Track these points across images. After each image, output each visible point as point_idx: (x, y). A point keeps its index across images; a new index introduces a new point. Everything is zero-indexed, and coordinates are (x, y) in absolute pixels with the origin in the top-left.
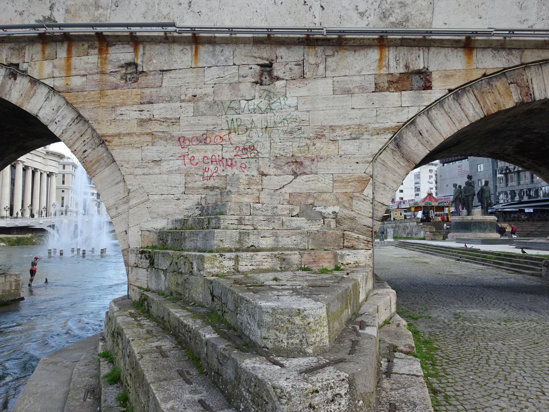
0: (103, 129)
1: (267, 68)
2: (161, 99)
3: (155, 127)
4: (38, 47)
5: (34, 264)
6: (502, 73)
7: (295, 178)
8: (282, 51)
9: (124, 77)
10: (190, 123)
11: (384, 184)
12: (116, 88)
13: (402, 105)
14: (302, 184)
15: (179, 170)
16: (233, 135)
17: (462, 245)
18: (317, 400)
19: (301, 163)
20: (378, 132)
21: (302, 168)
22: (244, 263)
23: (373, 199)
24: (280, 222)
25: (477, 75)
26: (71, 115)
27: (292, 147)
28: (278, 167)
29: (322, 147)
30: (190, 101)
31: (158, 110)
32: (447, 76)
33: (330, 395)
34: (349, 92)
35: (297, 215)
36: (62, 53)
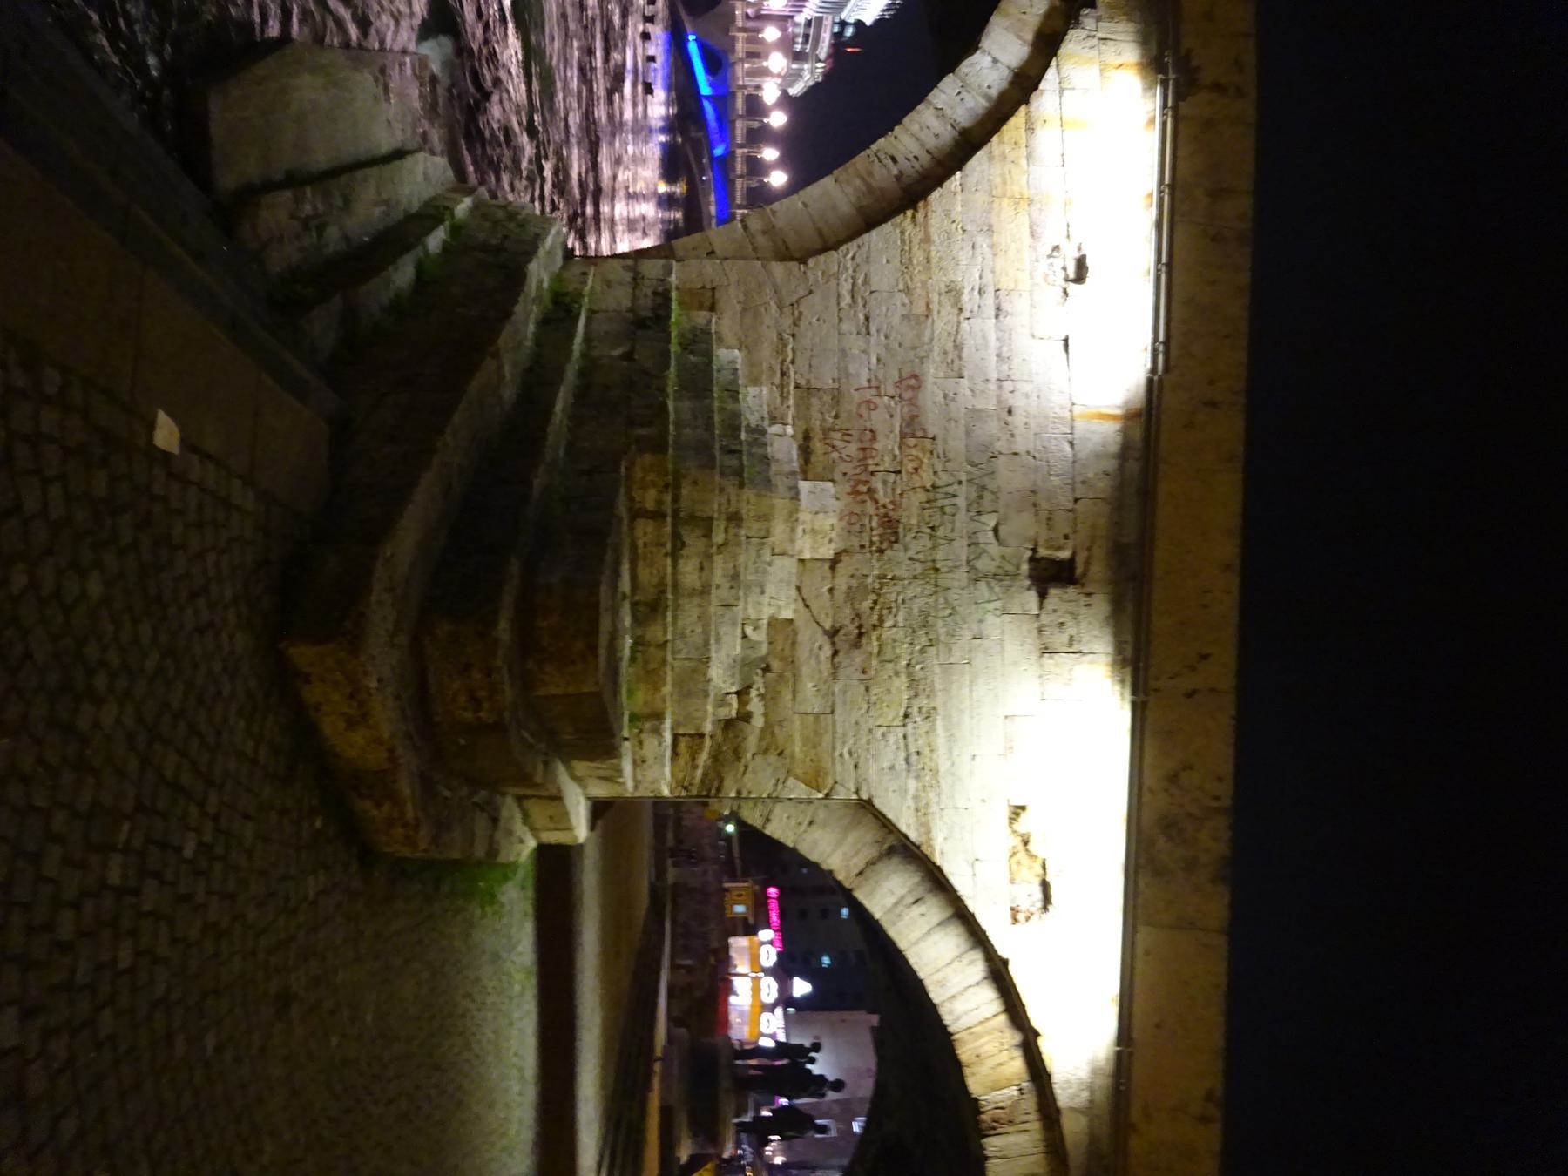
7: (826, 632)
11: (811, 823)
12: (1032, 234)
15: (848, 375)
16: (922, 496)
17: (659, 1052)
18: (477, 675)
19: (857, 645)
21: (847, 646)
22: (650, 529)
23: (777, 800)
24: (732, 601)
28: (851, 595)
30: (999, 402)
33: (482, 694)
35: (744, 636)
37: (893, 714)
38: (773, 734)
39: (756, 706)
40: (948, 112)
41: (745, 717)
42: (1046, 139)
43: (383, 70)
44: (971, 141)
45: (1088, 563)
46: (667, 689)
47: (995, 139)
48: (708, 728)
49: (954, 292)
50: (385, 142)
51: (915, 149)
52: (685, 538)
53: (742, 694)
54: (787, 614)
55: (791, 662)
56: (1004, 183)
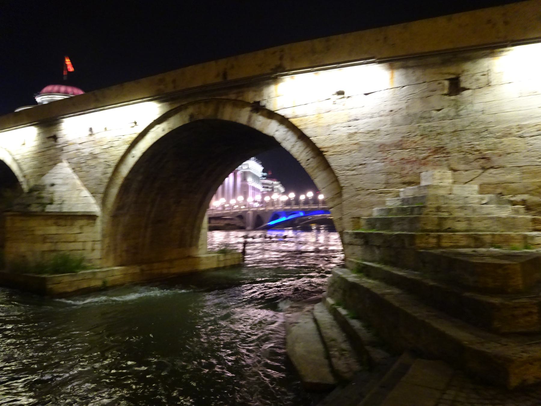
28: (468, 163)
30: (387, 116)
37: (520, 143)
38: (531, 191)
39: (519, 198)
40: (292, 144)
41: (523, 202)
42: (298, 111)
43: (291, 323)
44: (302, 136)
45: (449, 74)
46: (512, 233)
47: (300, 128)
48: (529, 217)
49: (350, 135)
50: (311, 325)
51: (304, 153)
52: (447, 227)
53: (514, 203)
54: (476, 187)
55: (498, 185)
56: (313, 123)
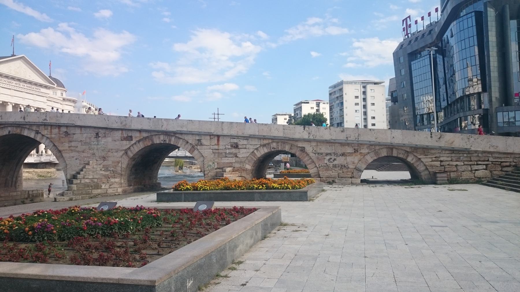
0: (60, 148)
1: (97, 134)
2: (73, 141)
3: (72, 148)
4: (43, 127)
5: (50, 186)
6: (147, 137)
8: (100, 130)
9: (65, 135)
10: (80, 148)
13: (126, 144)
14: (105, 163)
20: (122, 151)
25: (142, 137)
26: (52, 145)
27: (103, 154)
29: (110, 154)
31: (73, 144)
32: (136, 138)
34: (115, 141)
36: (49, 128)
